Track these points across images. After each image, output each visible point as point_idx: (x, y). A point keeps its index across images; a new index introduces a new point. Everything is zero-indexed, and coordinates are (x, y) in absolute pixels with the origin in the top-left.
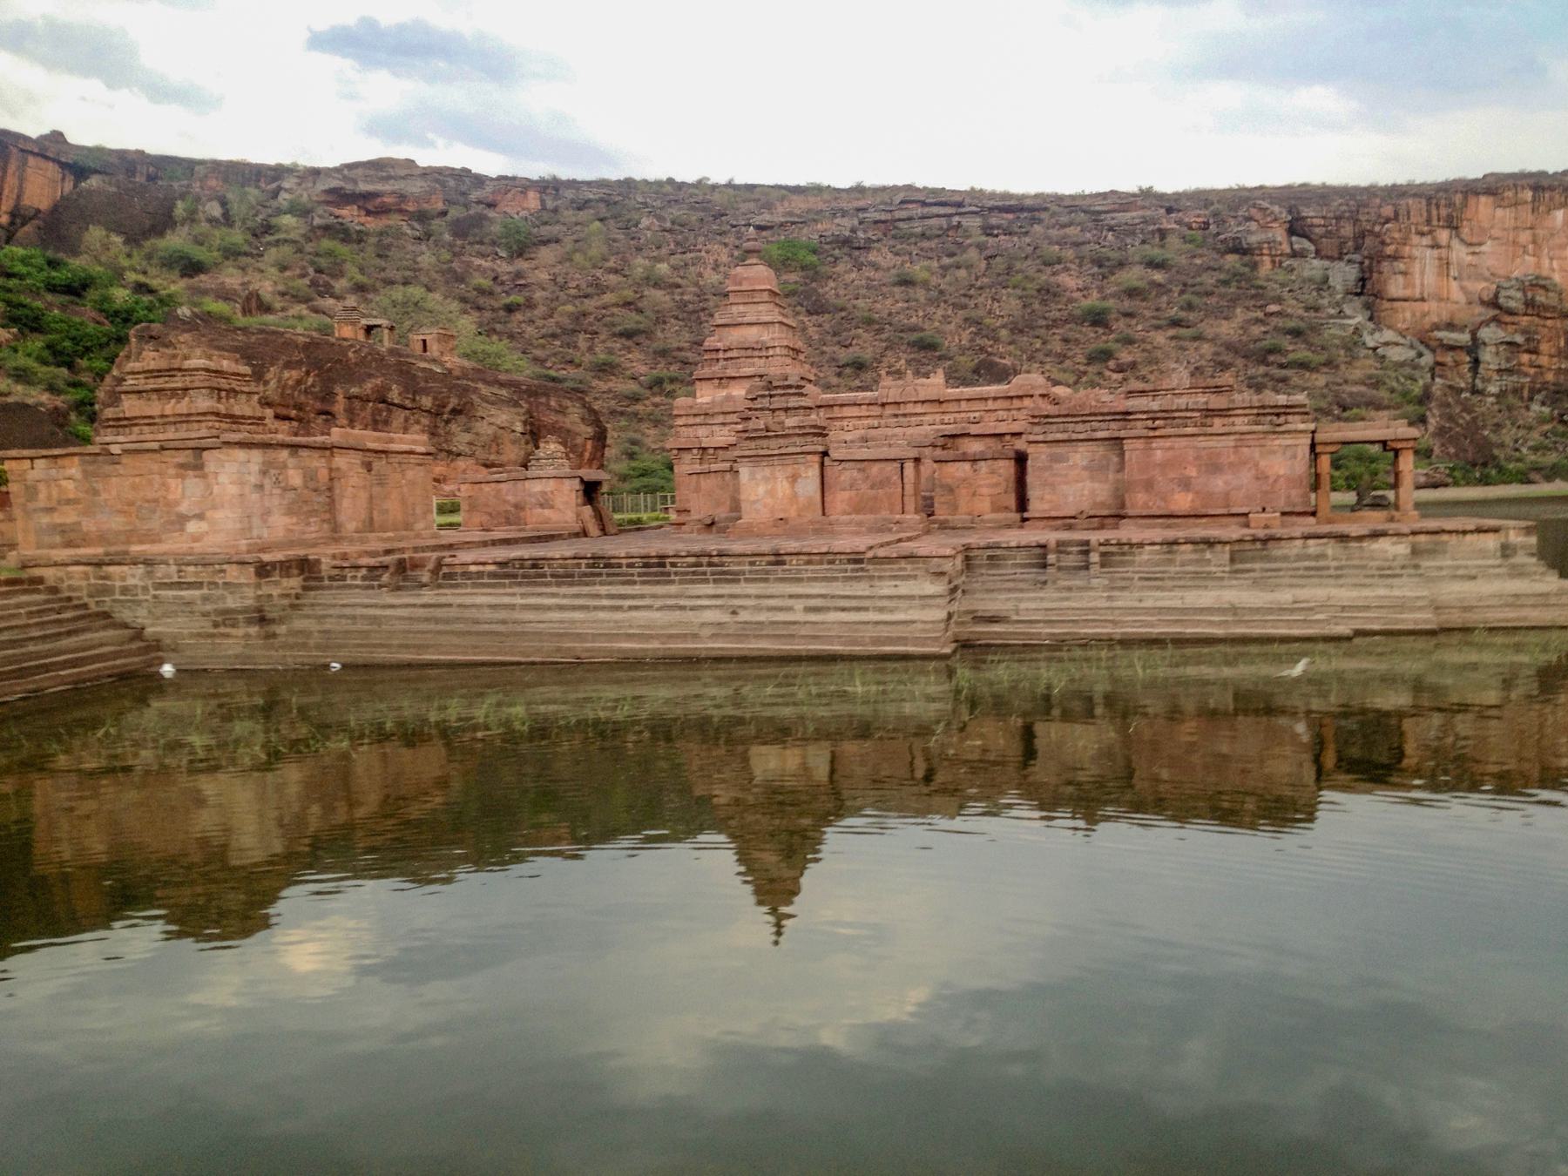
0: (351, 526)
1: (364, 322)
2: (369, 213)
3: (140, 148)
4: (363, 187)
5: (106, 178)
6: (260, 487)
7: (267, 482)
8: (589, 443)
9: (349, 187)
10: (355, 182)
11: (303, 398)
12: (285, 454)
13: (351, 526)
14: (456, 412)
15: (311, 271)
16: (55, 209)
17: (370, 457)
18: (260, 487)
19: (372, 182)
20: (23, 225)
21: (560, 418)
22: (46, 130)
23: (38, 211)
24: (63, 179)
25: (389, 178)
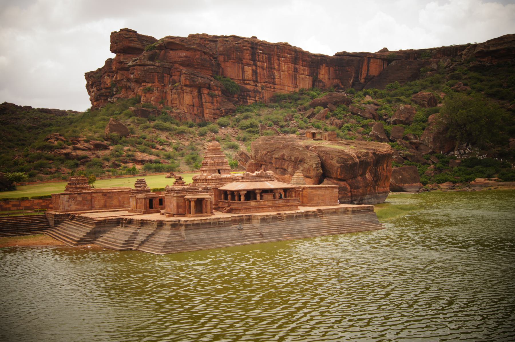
1: (312, 132)
3: (411, 49)
6: (68, 201)
7: (70, 200)
8: (339, 170)
9: (486, 50)
10: (489, 47)
11: (265, 159)
12: (76, 195)
14: (301, 161)
16: (380, 74)
18: (68, 201)
20: (369, 81)
21: (332, 161)
22: (382, 48)
23: (374, 76)
24: (383, 64)
25: (504, 43)
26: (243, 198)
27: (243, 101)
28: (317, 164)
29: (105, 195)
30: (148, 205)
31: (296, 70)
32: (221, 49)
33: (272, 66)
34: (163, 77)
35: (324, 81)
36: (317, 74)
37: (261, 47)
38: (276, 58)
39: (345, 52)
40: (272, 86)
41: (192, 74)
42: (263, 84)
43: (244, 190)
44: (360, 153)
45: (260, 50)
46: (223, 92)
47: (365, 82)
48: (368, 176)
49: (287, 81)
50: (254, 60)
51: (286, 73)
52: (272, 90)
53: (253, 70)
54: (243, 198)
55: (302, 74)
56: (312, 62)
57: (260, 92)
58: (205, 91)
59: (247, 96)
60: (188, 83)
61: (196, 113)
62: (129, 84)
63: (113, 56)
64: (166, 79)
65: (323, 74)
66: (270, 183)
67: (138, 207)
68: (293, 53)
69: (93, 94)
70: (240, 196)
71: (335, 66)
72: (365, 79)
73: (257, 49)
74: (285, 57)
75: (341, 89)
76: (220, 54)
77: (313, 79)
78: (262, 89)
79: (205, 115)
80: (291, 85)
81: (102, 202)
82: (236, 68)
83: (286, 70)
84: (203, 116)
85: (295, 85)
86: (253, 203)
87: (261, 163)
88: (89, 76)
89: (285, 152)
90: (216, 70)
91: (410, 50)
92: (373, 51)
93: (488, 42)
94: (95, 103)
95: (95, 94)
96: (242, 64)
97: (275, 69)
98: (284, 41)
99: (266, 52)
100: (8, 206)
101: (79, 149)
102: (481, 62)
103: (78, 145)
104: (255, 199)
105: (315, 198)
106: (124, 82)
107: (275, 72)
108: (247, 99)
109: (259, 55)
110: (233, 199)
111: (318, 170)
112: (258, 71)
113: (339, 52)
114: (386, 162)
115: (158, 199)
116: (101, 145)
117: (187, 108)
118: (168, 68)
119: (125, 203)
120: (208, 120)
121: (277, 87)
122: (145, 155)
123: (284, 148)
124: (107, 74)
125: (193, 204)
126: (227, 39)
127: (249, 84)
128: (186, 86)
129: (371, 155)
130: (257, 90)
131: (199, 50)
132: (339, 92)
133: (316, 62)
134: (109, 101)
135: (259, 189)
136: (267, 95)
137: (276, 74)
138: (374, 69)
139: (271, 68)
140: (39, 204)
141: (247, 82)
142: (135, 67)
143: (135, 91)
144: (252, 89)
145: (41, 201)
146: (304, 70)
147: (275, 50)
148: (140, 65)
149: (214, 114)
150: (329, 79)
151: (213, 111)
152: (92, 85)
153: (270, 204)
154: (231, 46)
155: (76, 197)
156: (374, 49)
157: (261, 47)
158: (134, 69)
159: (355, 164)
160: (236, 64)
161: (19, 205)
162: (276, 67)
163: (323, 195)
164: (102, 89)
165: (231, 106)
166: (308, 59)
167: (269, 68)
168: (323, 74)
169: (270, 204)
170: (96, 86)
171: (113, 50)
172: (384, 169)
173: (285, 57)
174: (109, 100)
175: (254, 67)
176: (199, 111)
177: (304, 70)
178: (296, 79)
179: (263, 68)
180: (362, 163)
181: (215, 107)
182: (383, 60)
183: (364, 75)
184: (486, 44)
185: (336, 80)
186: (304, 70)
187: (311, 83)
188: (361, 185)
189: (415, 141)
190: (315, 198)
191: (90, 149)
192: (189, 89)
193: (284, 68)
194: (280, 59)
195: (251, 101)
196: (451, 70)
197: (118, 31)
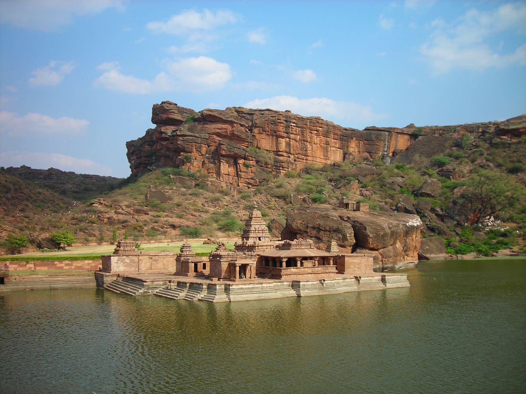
0: (144, 269)
2: (516, 136)
4: (511, 127)
5: (424, 137)
9: (506, 128)
10: (508, 126)
11: (301, 228)
13: (144, 269)
15: (484, 161)
16: (407, 149)
17: (151, 257)
19: (516, 125)
20: (397, 155)
23: (402, 150)
26: (284, 264)
27: (276, 171)
28: (351, 234)
29: (151, 259)
30: (193, 269)
31: (327, 143)
32: (257, 122)
33: (305, 139)
34: (201, 147)
35: (354, 153)
36: (348, 147)
37: (294, 121)
38: (308, 131)
39: (374, 127)
40: (305, 158)
41: (228, 145)
42: (296, 156)
43: (285, 258)
44: (391, 223)
45: (294, 123)
46: (257, 162)
47: (393, 155)
48: (398, 245)
49: (319, 153)
50: (287, 133)
51: (318, 145)
52: (304, 161)
53: (286, 142)
54: (284, 264)
55: (333, 147)
56: (343, 136)
57: (292, 164)
58: (241, 161)
59: (280, 167)
60: (224, 153)
61: (231, 182)
62: (168, 153)
63: (154, 126)
64: (204, 149)
65: (353, 147)
66: (310, 251)
67: (183, 271)
68: (325, 127)
69: (133, 162)
70: (281, 263)
71: (365, 140)
72: (393, 153)
73: (290, 122)
74: (317, 131)
75: (370, 161)
76: (256, 127)
77: (344, 152)
78: (295, 161)
79: (240, 184)
80: (322, 157)
81: (148, 265)
82: (271, 140)
83: (318, 142)
84: (238, 186)
85: (326, 157)
86: (293, 270)
87: (297, 231)
88: (129, 145)
89: (321, 222)
90: (251, 141)
91: (436, 126)
92: (401, 128)
93: (508, 121)
94: (134, 171)
95: (135, 162)
96: (276, 136)
97: (307, 141)
98: (316, 115)
99: (299, 125)
100: (61, 265)
101: (120, 213)
102: (502, 139)
103: (120, 210)
104: (296, 265)
105: (351, 266)
106: (163, 151)
107: (308, 144)
108: (280, 170)
109: (292, 128)
110: (275, 265)
111: (351, 239)
112: (291, 143)
113: (369, 126)
114: (415, 233)
115: (202, 263)
116: (142, 210)
117: (223, 178)
118: (206, 139)
119: (170, 266)
120: (242, 189)
121: (309, 158)
122: (181, 220)
123: (319, 218)
124: (147, 143)
125: (238, 269)
126: (262, 113)
127: (283, 156)
128: (223, 156)
129: (401, 226)
130: (290, 161)
131: (236, 123)
132: (368, 164)
133: (346, 136)
134: (149, 169)
135: (300, 257)
136: (300, 166)
137: (308, 146)
138: (402, 143)
139: (304, 141)
140: (88, 264)
141: (281, 153)
142: (175, 138)
143: (174, 160)
144: (285, 160)
145: (91, 262)
146: (334, 143)
147: (308, 124)
148: (180, 136)
149: (249, 183)
150: (359, 152)
151: (247, 180)
152: (133, 153)
153: (310, 271)
154: (266, 119)
155: (125, 259)
156: (401, 125)
157: (294, 121)
158: (174, 139)
159: (385, 235)
160: (271, 137)
161: (72, 265)
162: (309, 140)
163: (359, 264)
164: (141, 157)
165: (265, 176)
166: (339, 132)
167: (301, 141)
168: (353, 147)
169: (310, 271)
170: (136, 155)
171: (154, 121)
172: (413, 240)
173: (317, 131)
174: (149, 167)
175: (287, 139)
176: (234, 181)
177: (336, 143)
178: (327, 151)
179: (296, 141)
180: (393, 233)
181: (249, 177)
182: (409, 135)
183: (392, 150)
184: (506, 123)
185: (366, 153)
186: (336, 143)
187: (342, 155)
188: (392, 255)
189: (441, 213)
190: (351, 266)
191: (130, 214)
192: (225, 159)
193: (316, 141)
194: (313, 132)
195: (284, 171)
196: (474, 146)
197: (160, 103)
